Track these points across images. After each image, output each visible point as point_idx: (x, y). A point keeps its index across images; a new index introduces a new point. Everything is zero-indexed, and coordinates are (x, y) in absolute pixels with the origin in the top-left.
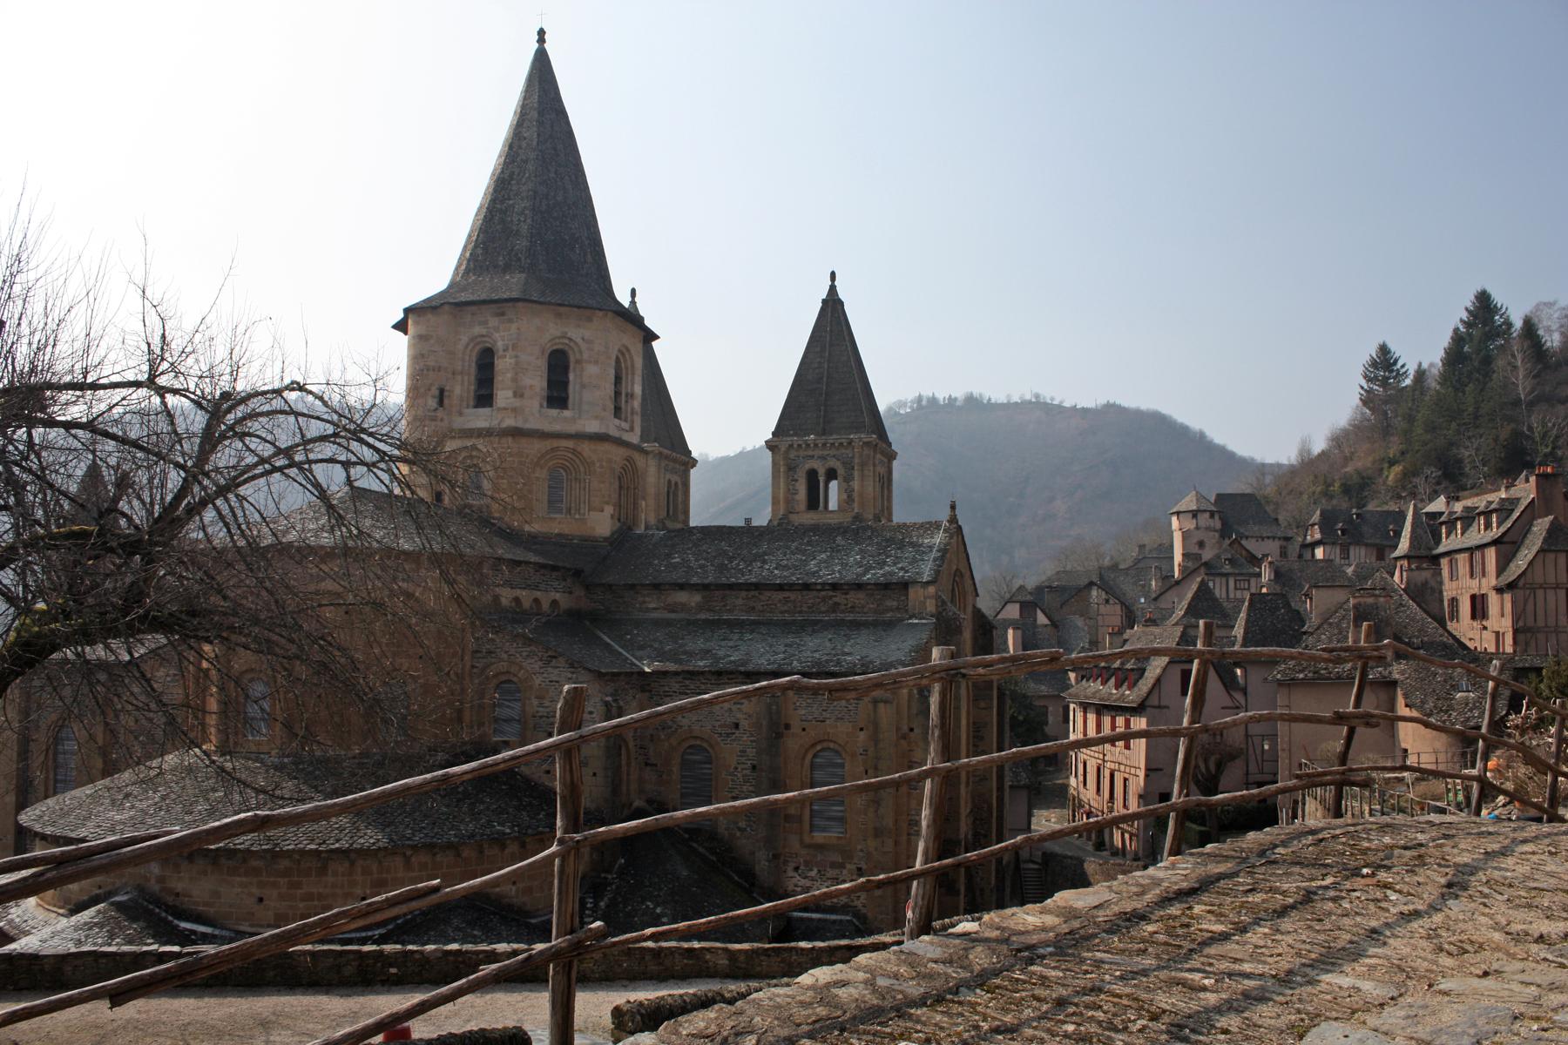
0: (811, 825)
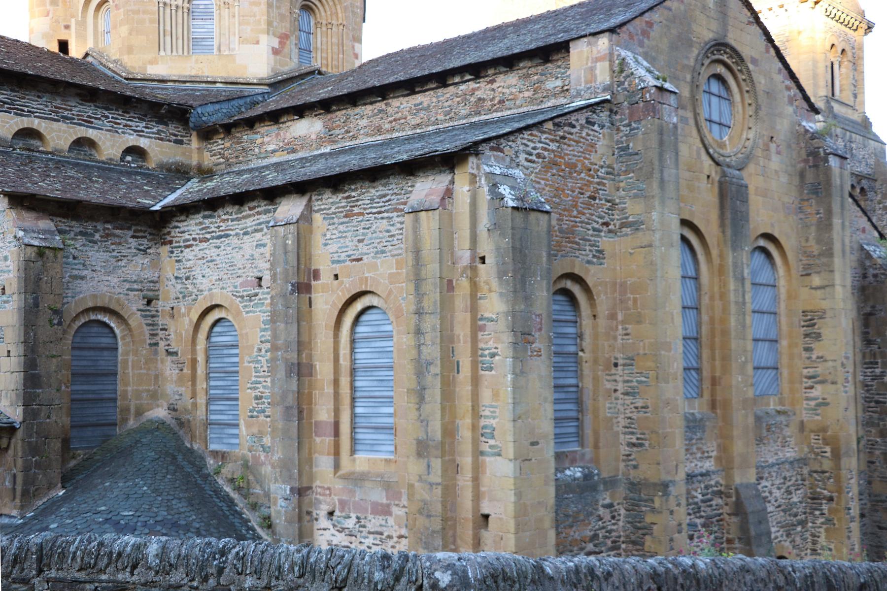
0: (354, 441)
